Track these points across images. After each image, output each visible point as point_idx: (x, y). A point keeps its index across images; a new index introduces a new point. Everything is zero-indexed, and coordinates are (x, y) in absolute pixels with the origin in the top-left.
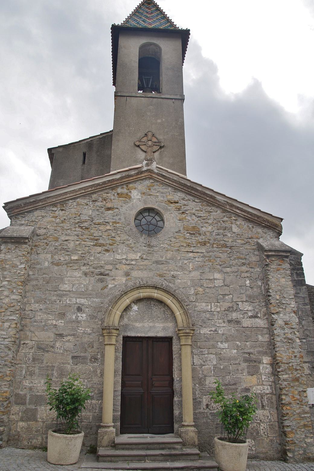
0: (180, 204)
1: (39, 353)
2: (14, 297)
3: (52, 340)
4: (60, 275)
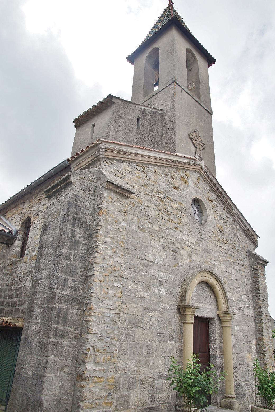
0: (213, 203)
1: (130, 328)
2: (117, 259)
3: (141, 314)
4: (145, 242)
